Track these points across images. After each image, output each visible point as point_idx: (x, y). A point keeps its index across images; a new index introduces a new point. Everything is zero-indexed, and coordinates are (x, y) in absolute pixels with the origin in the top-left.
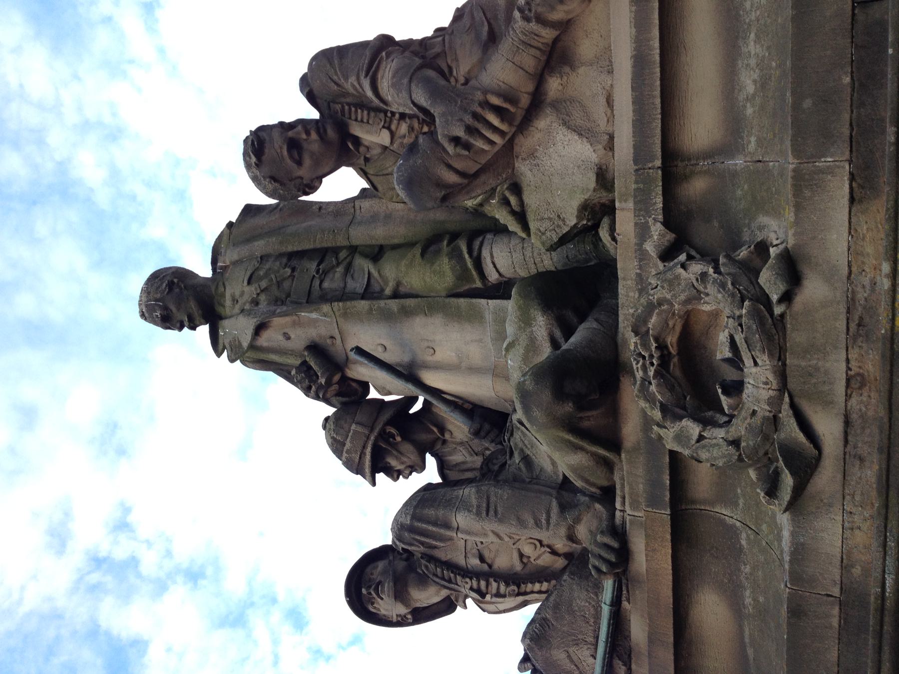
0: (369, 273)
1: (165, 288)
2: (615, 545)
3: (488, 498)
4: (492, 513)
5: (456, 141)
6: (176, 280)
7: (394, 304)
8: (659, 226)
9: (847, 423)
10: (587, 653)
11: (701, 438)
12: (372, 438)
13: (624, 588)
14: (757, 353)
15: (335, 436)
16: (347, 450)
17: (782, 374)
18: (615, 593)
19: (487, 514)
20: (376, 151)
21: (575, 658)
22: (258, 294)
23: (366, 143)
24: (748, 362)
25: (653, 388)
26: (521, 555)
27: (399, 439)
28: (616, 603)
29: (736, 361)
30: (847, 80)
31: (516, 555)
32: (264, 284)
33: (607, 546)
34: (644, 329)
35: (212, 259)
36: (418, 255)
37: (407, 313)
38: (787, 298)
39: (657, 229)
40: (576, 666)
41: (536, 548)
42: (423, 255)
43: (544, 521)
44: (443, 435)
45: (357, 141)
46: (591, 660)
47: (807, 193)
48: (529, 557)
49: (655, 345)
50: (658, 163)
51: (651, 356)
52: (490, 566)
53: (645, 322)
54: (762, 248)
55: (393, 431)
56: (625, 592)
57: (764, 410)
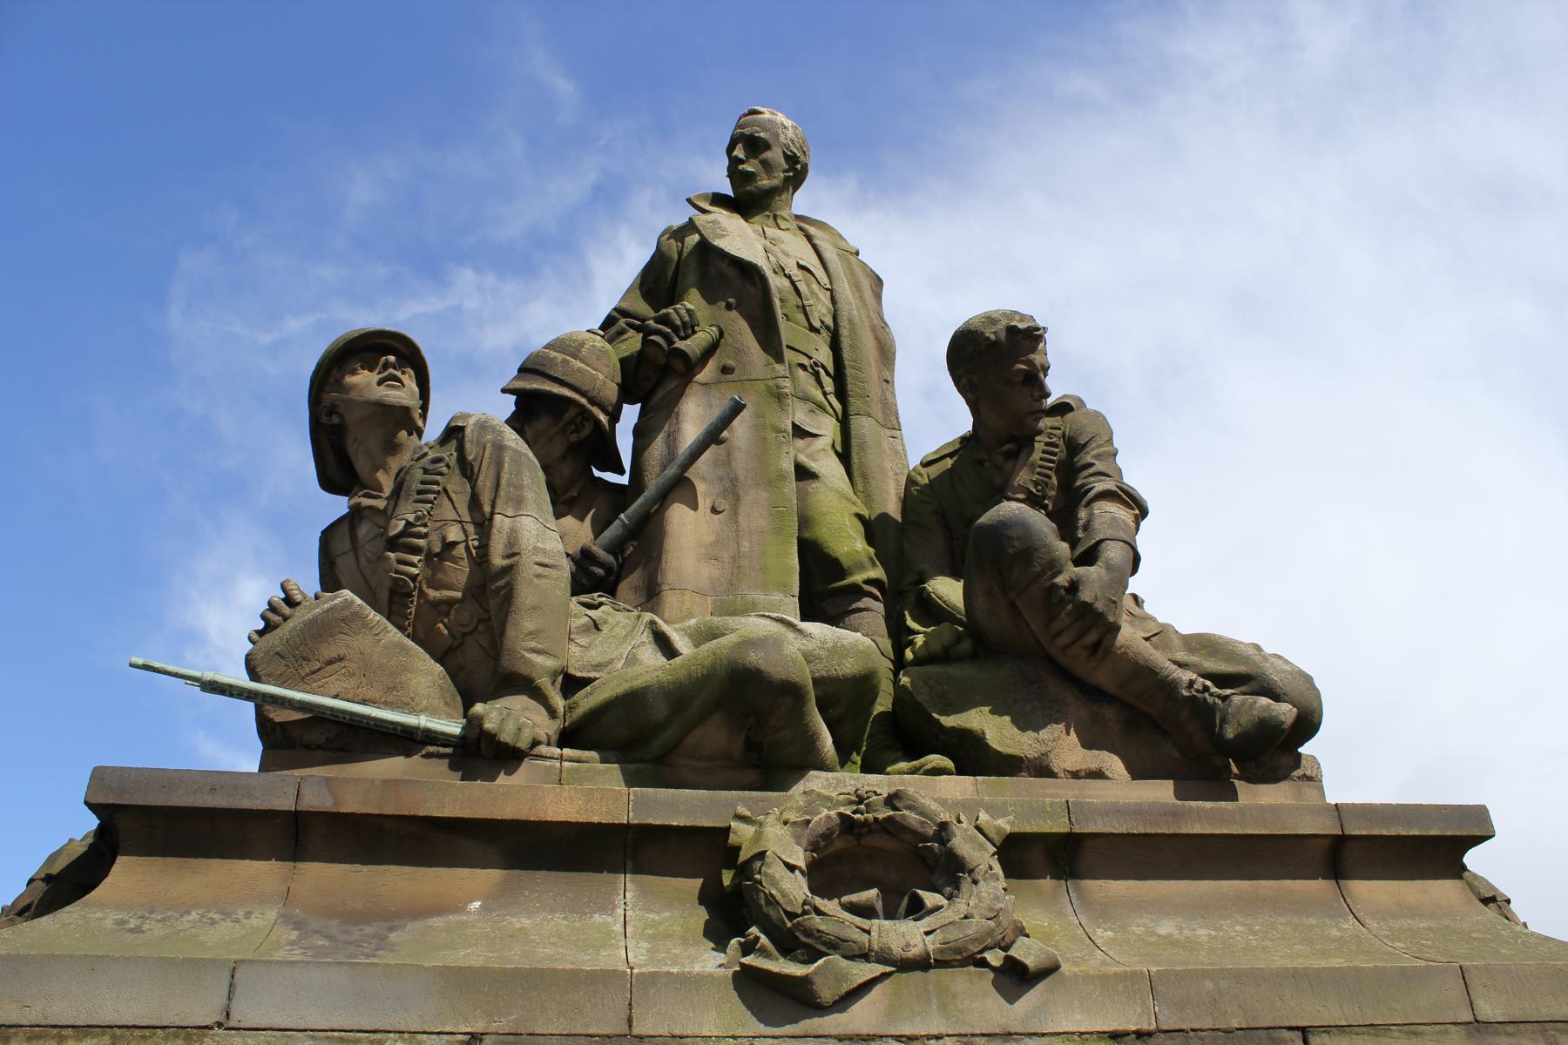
1: (791, 151)
6: (799, 166)
10: (338, 687)
12: (584, 401)
16: (568, 362)
17: (922, 964)
18: (441, 737)
21: (331, 668)
22: (789, 277)
27: (574, 438)
32: (802, 287)
34: (898, 804)
40: (319, 670)
41: (464, 626)
43: (533, 644)
47: (1120, 988)
53: (909, 808)
55: (586, 432)
56: (441, 750)
57: (876, 942)
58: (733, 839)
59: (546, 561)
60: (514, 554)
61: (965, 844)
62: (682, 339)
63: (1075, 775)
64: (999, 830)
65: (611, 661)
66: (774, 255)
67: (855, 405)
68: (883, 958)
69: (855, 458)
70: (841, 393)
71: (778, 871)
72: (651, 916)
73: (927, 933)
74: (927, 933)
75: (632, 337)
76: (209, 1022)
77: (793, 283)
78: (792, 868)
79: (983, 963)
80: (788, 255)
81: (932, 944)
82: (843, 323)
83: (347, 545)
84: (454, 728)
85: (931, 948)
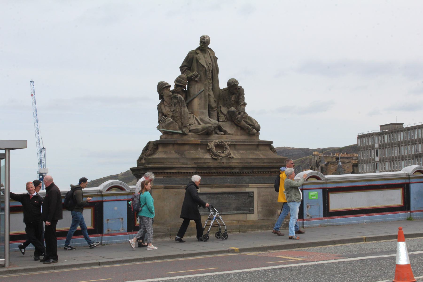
5: (238, 118)
20: (231, 97)
22: (208, 65)
24: (224, 154)
26: (177, 117)
28: (179, 133)
31: (177, 116)
36: (214, 100)
39: (229, 143)
45: (233, 95)
46: (171, 129)
57: (221, 155)
58: (208, 145)
60: (185, 113)
61: (228, 148)
63: (235, 135)
64: (229, 144)
67: (214, 82)
68: (221, 156)
69: (214, 89)
71: (213, 149)
75: (187, 71)
78: (214, 149)
79: (228, 157)
80: (208, 61)
81: (225, 156)
82: (213, 70)
84: (181, 132)
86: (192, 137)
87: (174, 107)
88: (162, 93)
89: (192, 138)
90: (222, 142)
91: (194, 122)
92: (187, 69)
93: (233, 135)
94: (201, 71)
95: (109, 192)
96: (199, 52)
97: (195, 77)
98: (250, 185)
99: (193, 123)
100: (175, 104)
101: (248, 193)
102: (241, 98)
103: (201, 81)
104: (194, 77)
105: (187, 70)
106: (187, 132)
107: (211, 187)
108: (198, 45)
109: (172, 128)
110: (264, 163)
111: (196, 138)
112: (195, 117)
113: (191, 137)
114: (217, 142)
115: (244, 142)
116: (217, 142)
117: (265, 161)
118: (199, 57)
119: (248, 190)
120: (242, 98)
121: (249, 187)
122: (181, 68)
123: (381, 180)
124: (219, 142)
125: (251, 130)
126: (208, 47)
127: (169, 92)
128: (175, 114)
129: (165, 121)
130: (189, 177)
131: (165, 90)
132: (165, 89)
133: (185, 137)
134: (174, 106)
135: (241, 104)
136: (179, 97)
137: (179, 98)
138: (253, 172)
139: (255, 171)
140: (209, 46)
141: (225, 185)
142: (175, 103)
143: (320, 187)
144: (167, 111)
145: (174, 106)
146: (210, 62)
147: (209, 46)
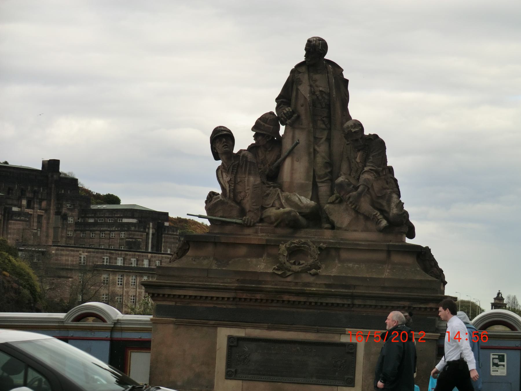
0: (322, 138)
2: (251, 225)
3: (258, 187)
4: (255, 189)
5: (349, 197)
7: (312, 150)
8: (326, 246)
9: (289, 282)
11: (284, 256)
13: (240, 225)
14: (301, 268)
15: (269, 120)
19: (254, 188)
22: (316, 95)
23: (358, 153)
24: (300, 266)
25: (293, 245)
28: (236, 223)
29: (299, 264)
30: (344, 284)
31: (240, 191)
32: (320, 98)
33: (251, 222)
35: (330, 61)
36: (326, 161)
37: (309, 154)
38: (310, 274)
39: (325, 246)
42: (326, 163)
44: (268, 151)
46: (219, 216)
48: (240, 194)
49: (302, 246)
50: (338, 247)
51: (299, 245)
52: (237, 184)
53: (306, 245)
54: (319, 268)
55: (270, 139)
59: (256, 187)
62: (289, 119)
64: (324, 247)
65: (270, 204)
66: (313, 88)
68: (292, 271)
70: (330, 122)
72: (268, 258)
73: (299, 268)
74: (299, 268)
75: (282, 107)
76: (206, 276)
77: (318, 97)
81: (300, 270)
83: (221, 176)
85: (299, 270)
86: (262, 231)
87: (232, 174)
88: (215, 149)
89: (262, 233)
90: (304, 243)
91: (274, 203)
92: (282, 101)
93: (346, 230)
94: (302, 106)
95: (75, 324)
96: (303, 69)
97: (286, 117)
98: (347, 329)
99: (271, 205)
100: (232, 169)
101: (343, 345)
102: (370, 159)
103: (302, 124)
104: (284, 118)
105: (283, 105)
106: (249, 222)
107: (269, 329)
108: (301, 58)
109: (220, 214)
110: (384, 288)
111: (269, 234)
112: (278, 194)
113: (259, 232)
114: (296, 243)
115: (358, 245)
116: (294, 243)
117: (386, 285)
118: (299, 79)
119: (344, 339)
120: (371, 157)
121: (346, 333)
122: (277, 101)
123: (494, 338)
124: (300, 242)
125: (378, 222)
126: (325, 58)
127: (223, 147)
128: (232, 188)
129: (211, 200)
130: (225, 307)
131: (218, 142)
132: (218, 140)
133: (248, 231)
134: (231, 172)
135: (364, 169)
136: (242, 155)
137: (241, 157)
138: (354, 305)
139: (357, 302)
140: (326, 57)
141: (294, 326)
142: (233, 167)
143: (514, 346)
144: (224, 181)
145: (232, 172)
146: (321, 89)
147: (326, 57)
